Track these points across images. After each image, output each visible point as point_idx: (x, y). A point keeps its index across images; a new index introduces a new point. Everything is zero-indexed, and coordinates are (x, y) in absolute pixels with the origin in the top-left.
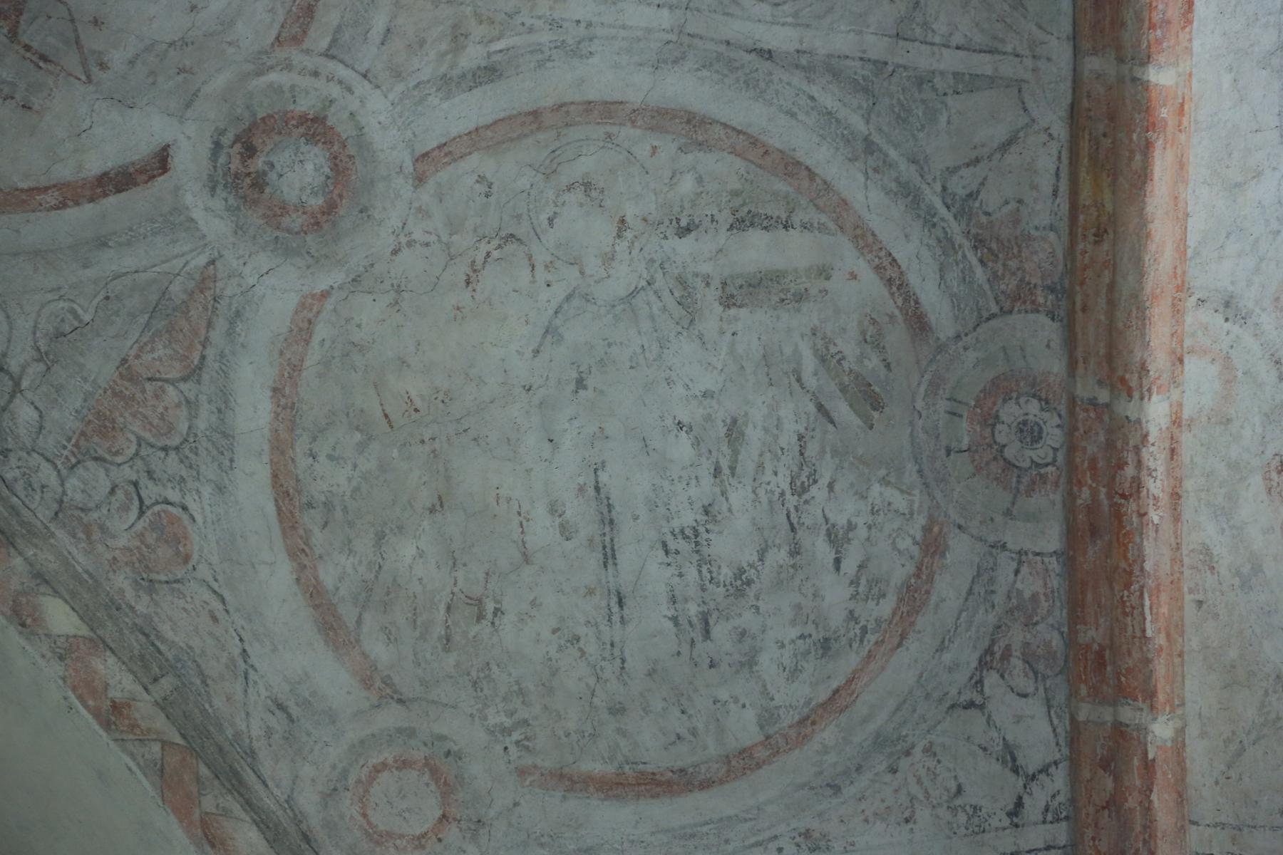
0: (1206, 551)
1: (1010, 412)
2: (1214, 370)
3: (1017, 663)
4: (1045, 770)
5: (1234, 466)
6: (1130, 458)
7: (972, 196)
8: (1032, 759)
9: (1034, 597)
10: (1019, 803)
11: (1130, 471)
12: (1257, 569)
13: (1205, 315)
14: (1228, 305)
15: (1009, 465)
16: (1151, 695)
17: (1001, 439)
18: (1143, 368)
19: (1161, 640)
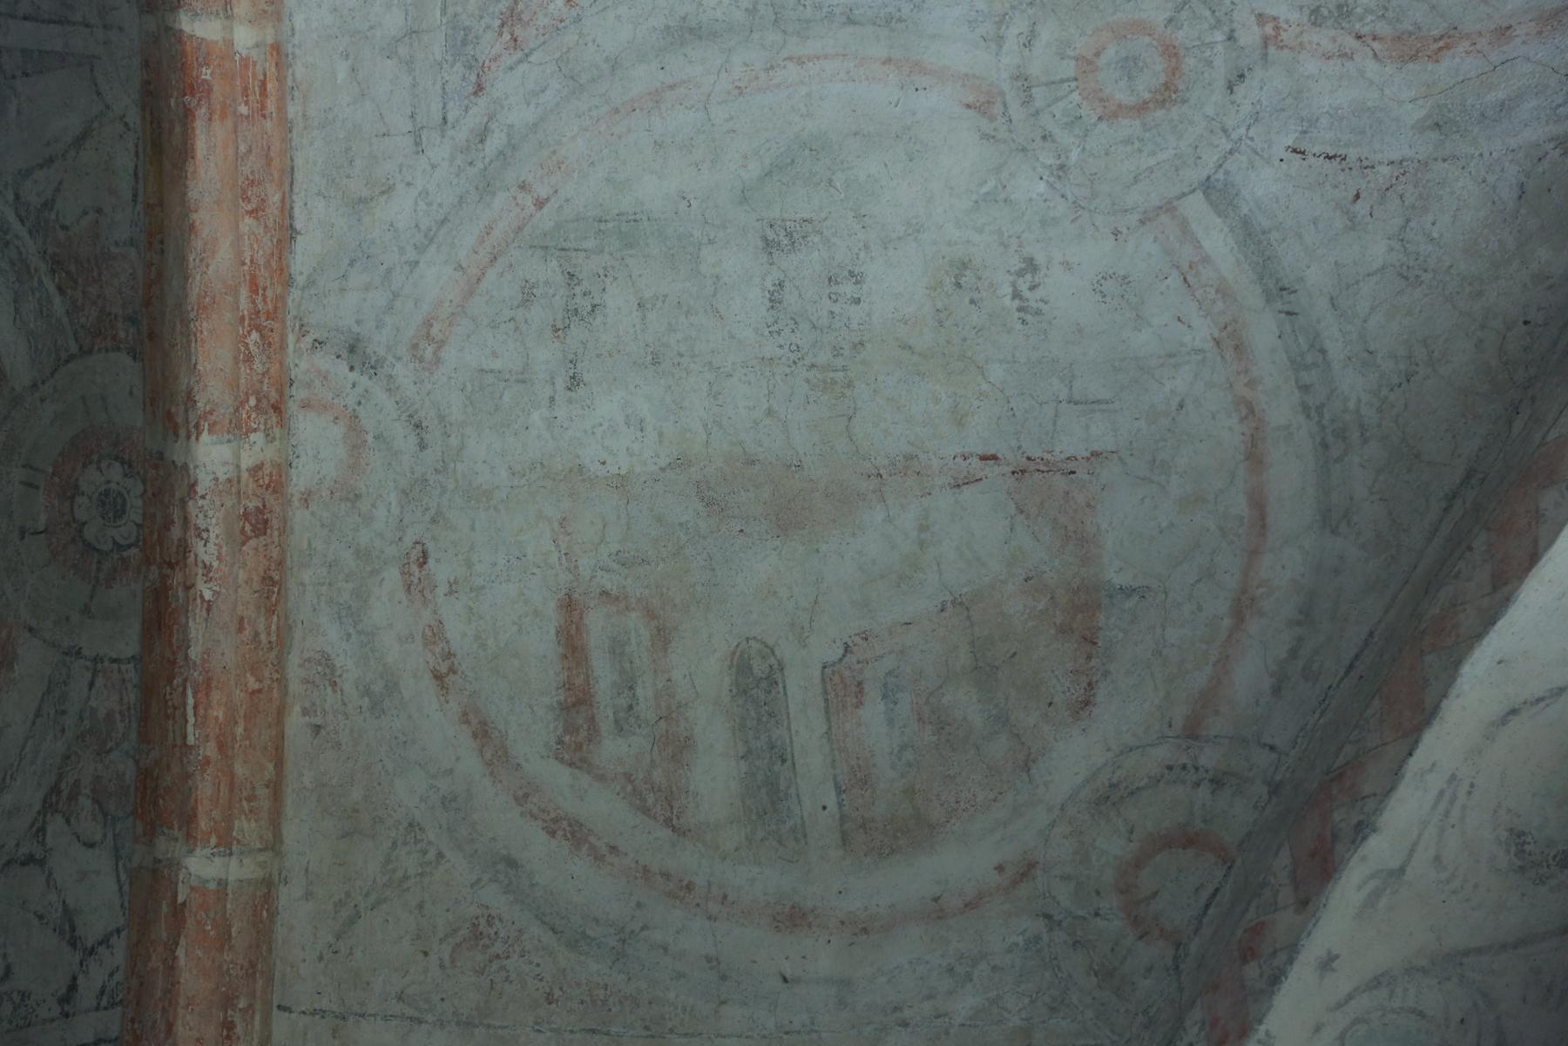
0: (326, 660)
1: (91, 480)
2: (338, 431)
3: (85, 802)
4: (105, 941)
5: (363, 554)
6: (176, 515)
7: (48, 205)
8: (92, 930)
9: (109, 716)
10: (73, 987)
11: (176, 532)
12: (392, 687)
13: (324, 361)
14: (354, 349)
15: (89, 547)
16: (189, 819)
17: (81, 515)
18: (190, 399)
19: (210, 750)
